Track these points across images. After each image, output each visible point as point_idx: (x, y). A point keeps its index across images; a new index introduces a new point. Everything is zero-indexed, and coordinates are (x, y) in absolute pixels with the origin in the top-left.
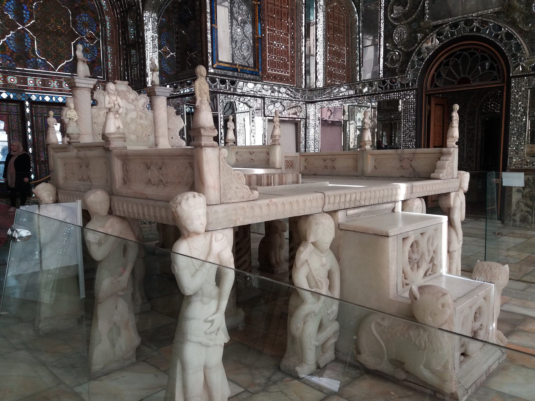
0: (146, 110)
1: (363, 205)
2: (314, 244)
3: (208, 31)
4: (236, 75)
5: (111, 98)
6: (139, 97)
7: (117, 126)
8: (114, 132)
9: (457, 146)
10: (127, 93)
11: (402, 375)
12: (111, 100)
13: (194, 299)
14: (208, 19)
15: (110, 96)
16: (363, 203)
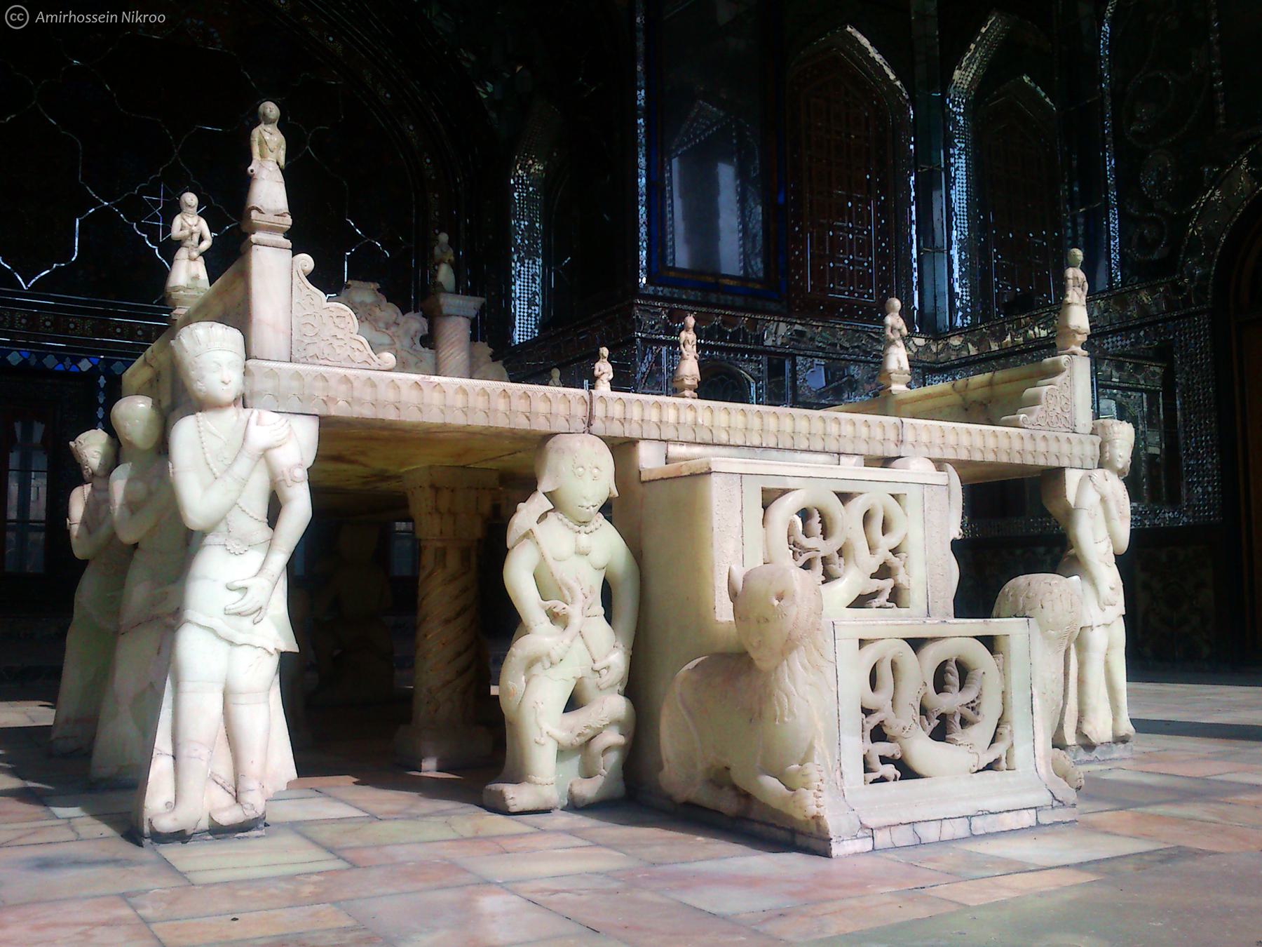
0: (418, 349)
1: (724, 442)
2: (550, 496)
3: (640, 198)
4: (714, 300)
5: (186, 222)
6: (402, 319)
8: (186, 286)
9: (1086, 353)
10: (374, 308)
11: (728, 804)
12: (185, 224)
13: (210, 539)
14: (639, 170)
15: (185, 217)
16: (724, 438)
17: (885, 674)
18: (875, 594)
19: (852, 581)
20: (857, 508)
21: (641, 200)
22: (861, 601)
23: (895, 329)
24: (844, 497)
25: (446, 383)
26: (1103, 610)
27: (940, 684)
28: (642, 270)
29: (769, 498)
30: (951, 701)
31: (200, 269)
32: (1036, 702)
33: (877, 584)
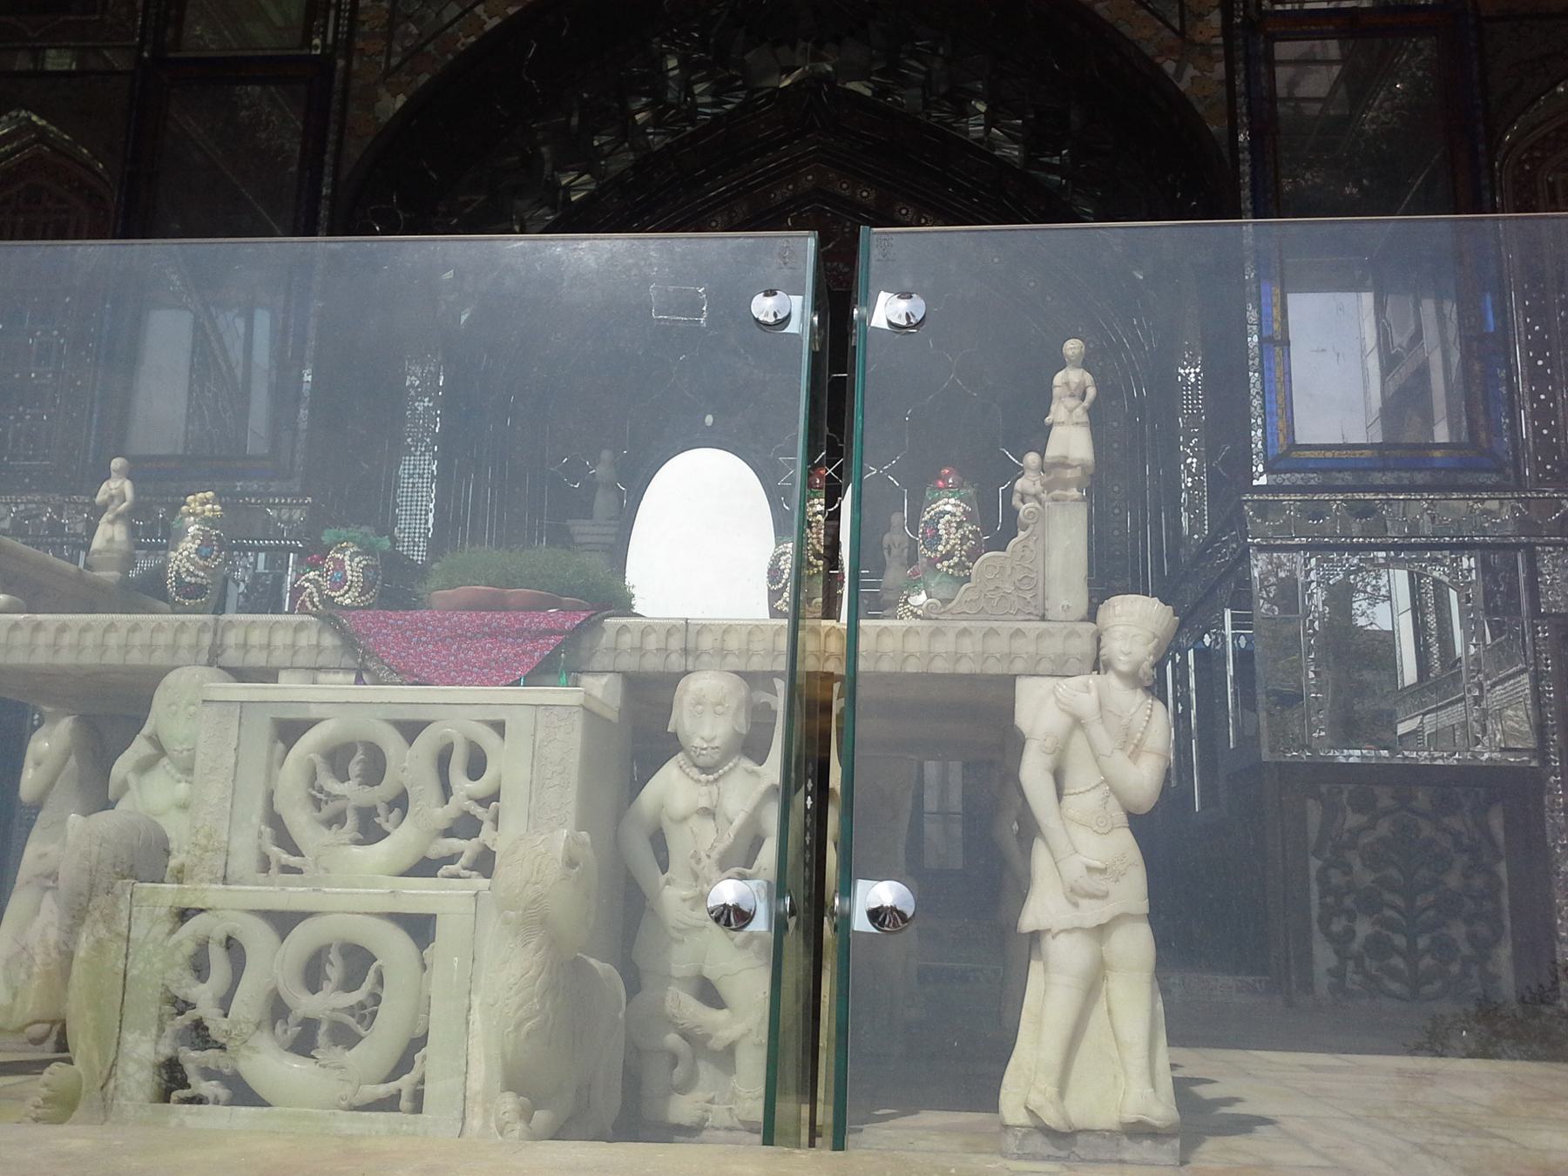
3: (1251, 362)
7: (109, 534)
14: (1249, 327)
17: (217, 956)
18: (452, 859)
19: (403, 840)
20: (426, 742)
21: (1253, 364)
22: (425, 867)
23: (1027, 494)
24: (410, 730)
25: (70, 620)
26: (1076, 905)
27: (313, 976)
28: (1257, 454)
29: (289, 731)
30: (327, 1003)
31: (119, 533)
32: (476, 1016)
33: (455, 844)
